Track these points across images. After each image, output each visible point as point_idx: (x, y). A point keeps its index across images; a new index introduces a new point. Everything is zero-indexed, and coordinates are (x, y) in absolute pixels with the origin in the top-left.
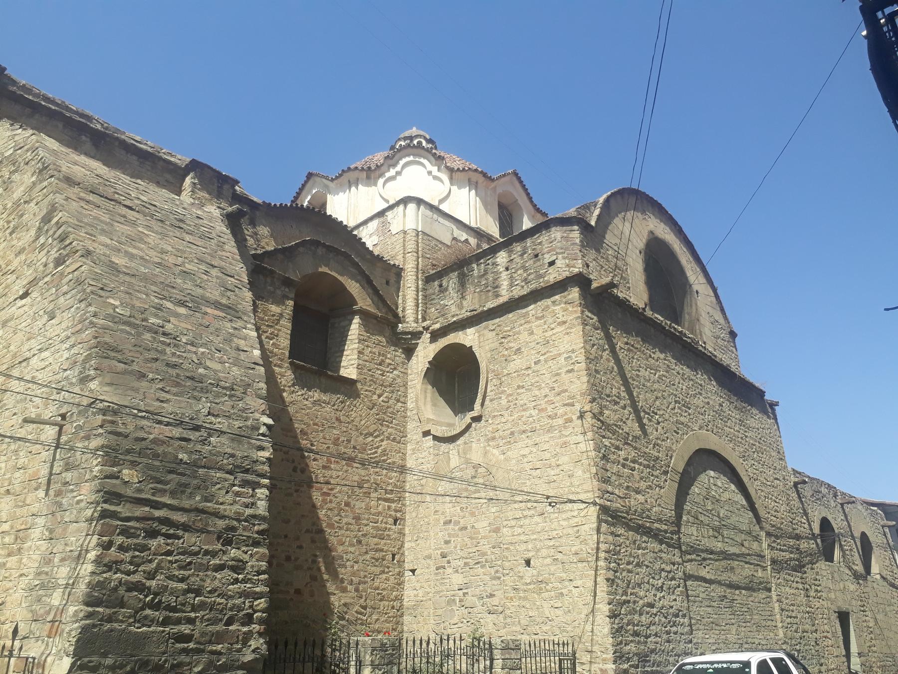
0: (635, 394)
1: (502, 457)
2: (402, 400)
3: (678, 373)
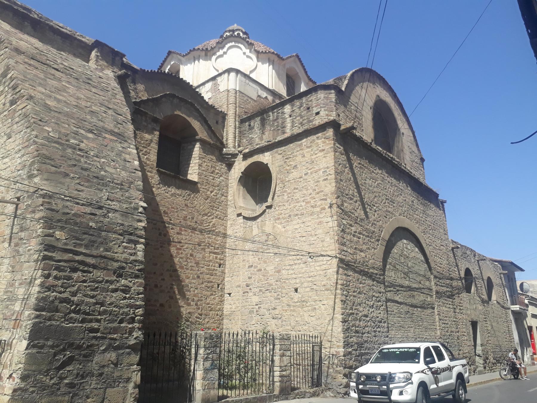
0: (363, 194)
1: (283, 230)
2: (225, 195)
3: (389, 182)
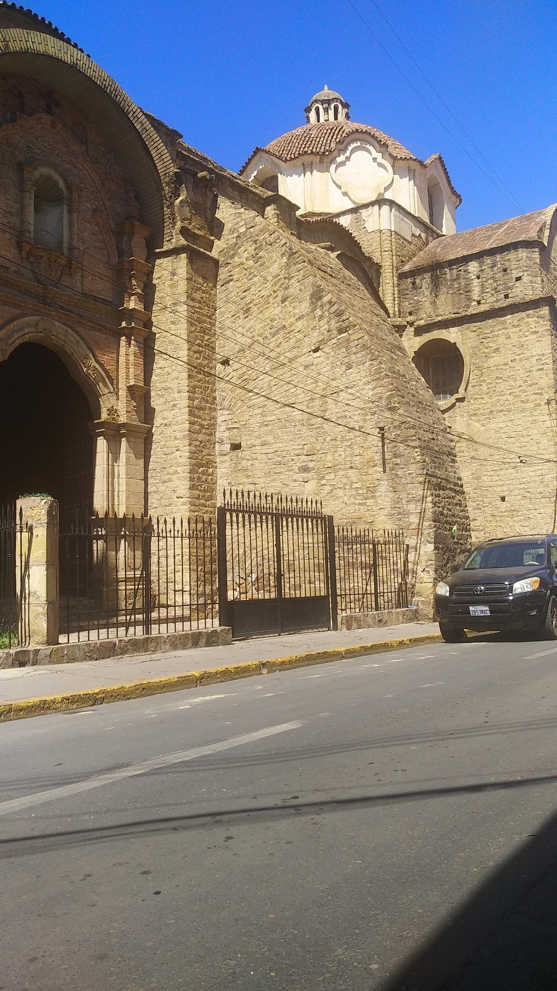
1: (483, 428)
